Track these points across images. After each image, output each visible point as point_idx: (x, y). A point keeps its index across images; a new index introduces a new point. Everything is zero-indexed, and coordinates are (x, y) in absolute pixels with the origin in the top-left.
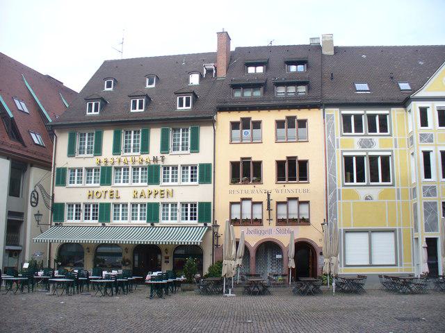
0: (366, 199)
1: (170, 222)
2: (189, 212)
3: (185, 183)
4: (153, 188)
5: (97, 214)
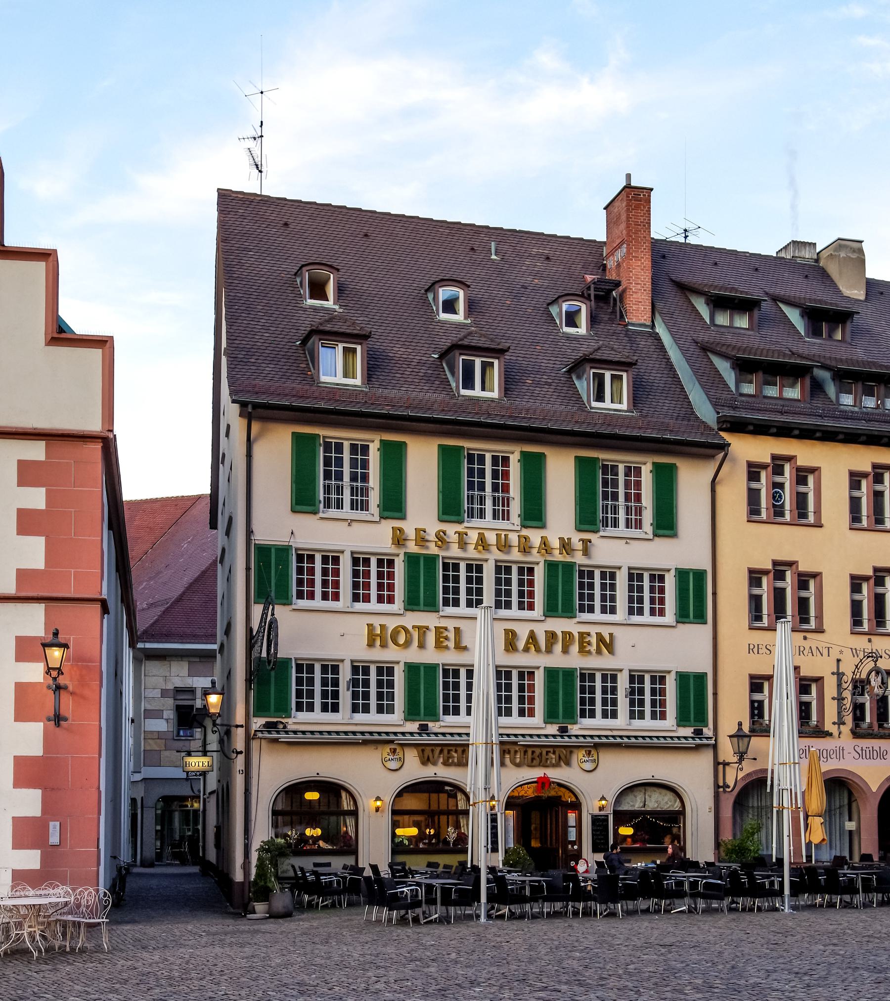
1: (622, 721)
3: (636, 619)
4: (559, 625)
5: (583, 691)
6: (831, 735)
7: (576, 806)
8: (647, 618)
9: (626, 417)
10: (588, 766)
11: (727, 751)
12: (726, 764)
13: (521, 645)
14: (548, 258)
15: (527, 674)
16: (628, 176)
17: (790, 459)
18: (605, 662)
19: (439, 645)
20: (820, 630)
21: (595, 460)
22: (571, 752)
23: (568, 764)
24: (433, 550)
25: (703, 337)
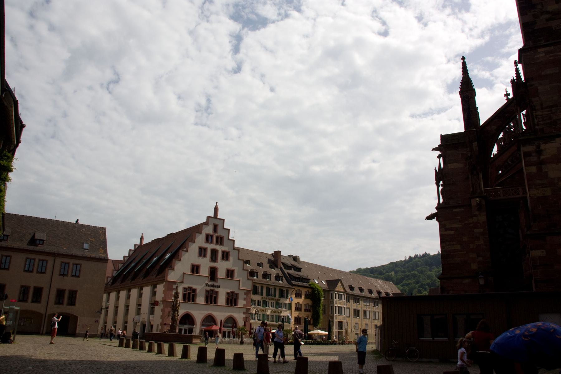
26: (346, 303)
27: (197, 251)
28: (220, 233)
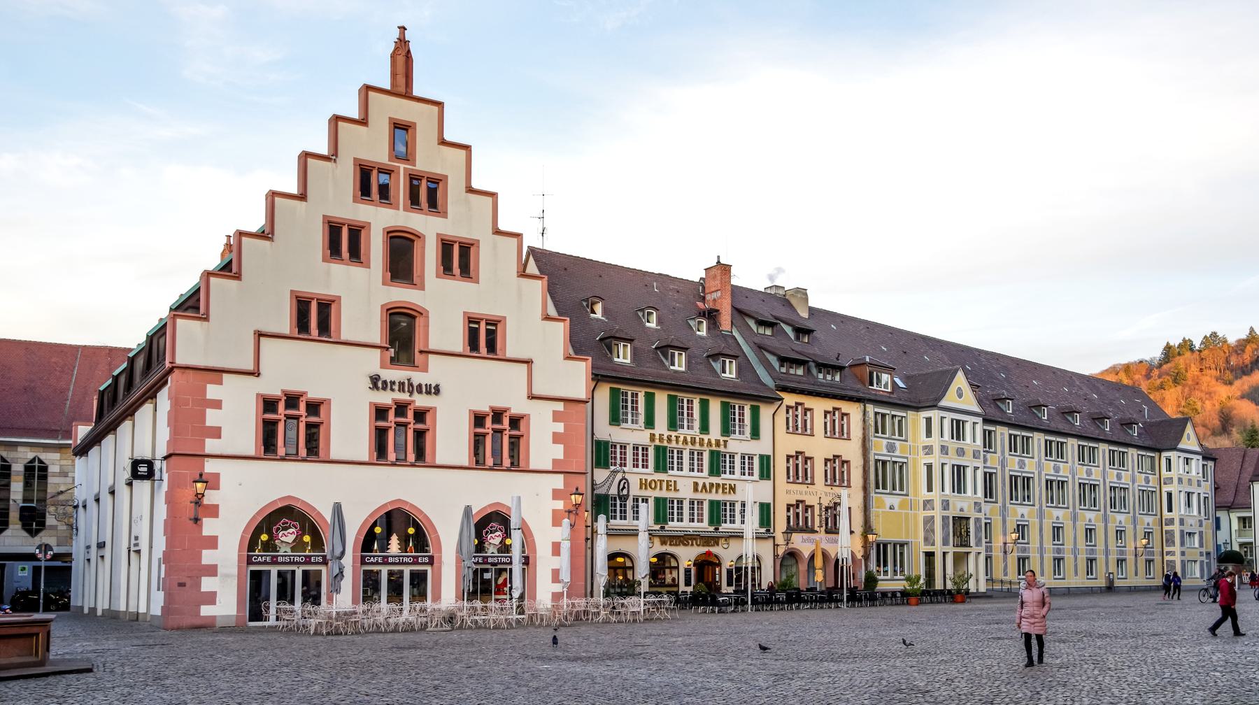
0: (891, 508)
2: (696, 512)
4: (715, 480)
6: (817, 532)
7: (719, 565)
8: (746, 477)
9: (734, 383)
10: (725, 546)
11: (780, 539)
12: (778, 545)
13: (700, 489)
14: (678, 292)
15: (700, 502)
16: (718, 257)
17: (801, 404)
18: (729, 497)
19: (668, 489)
20: (813, 484)
21: (729, 402)
22: (719, 540)
23: (718, 545)
24: (665, 444)
25: (757, 340)
26: (982, 453)
27: (318, 238)
28: (428, 160)
